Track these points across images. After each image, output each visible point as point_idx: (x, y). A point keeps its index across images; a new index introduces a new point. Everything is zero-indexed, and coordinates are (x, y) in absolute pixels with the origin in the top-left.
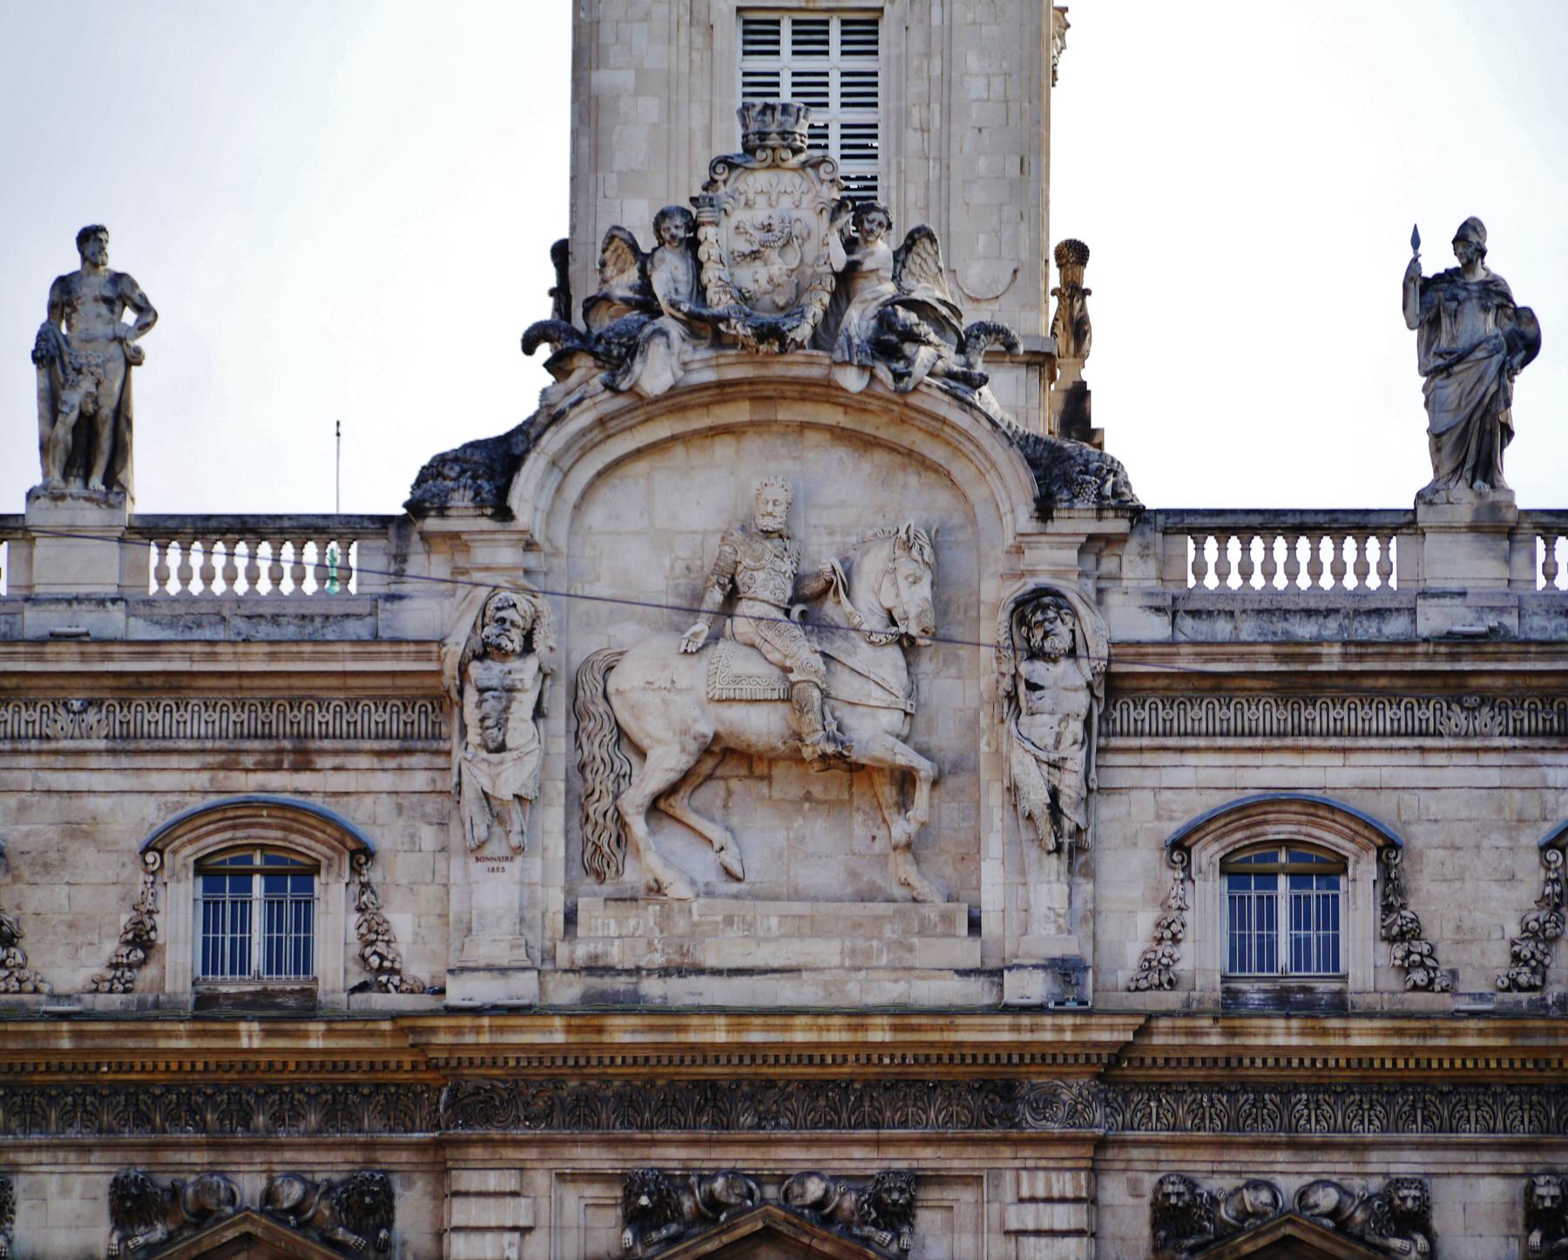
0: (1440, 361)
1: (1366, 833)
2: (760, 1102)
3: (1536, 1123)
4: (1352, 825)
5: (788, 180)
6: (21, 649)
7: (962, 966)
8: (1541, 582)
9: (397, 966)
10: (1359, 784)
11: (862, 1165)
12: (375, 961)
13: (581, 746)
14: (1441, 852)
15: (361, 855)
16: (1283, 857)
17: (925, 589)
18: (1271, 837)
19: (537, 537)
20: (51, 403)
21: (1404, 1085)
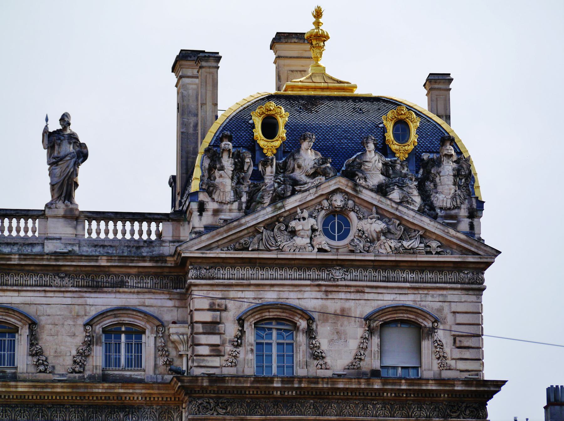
0: (54, 160)
1: (25, 319)
3: (80, 418)
4: (21, 316)
8: (87, 236)
10: (23, 302)
14: (50, 326)
21: (35, 405)
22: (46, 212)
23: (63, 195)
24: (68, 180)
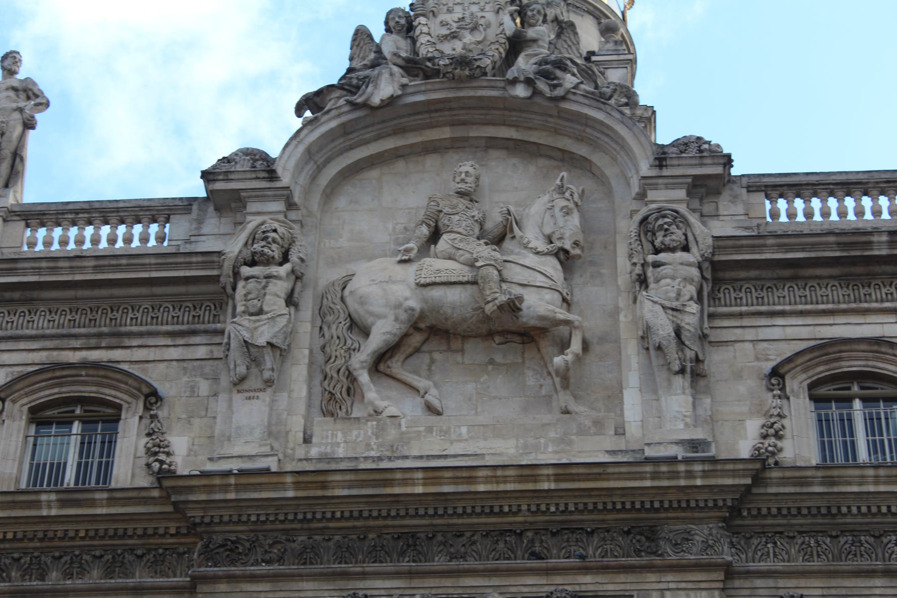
2: (451, 545)
9: (173, 468)
11: (534, 589)
12: (156, 466)
13: (323, 336)
15: (152, 398)
16: (855, 389)
17: (575, 220)
18: (846, 370)
19: (296, 199)
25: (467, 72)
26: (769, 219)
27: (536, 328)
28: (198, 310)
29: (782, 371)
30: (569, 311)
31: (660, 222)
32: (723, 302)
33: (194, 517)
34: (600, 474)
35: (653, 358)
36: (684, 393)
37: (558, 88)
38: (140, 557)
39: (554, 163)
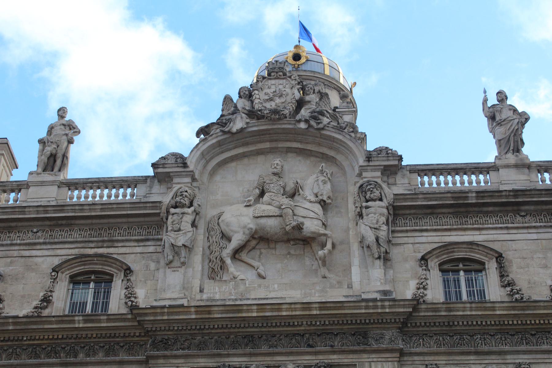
1: (491, 253)
2: (270, 341)
4: (486, 251)
5: (281, 81)
6: (17, 210)
7: (345, 295)
8: (541, 183)
9: (137, 304)
10: (486, 240)
11: (309, 362)
12: (130, 303)
13: (209, 241)
14: (519, 260)
15: (128, 271)
16: (461, 266)
17: (328, 186)
18: (456, 257)
20: (42, 152)
22: (496, 163)
23: (511, 148)
24: (514, 136)
25: (277, 117)
26: (420, 186)
27: (310, 238)
28: (150, 229)
29: (426, 258)
30: (326, 229)
31: (369, 187)
32: (398, 225)
33: (148, 328)
34: (340, 307)
35: (366, 252)
36: (380, 268)
37: (320, 124)
38: (122, 347)
39: (318, 159)
